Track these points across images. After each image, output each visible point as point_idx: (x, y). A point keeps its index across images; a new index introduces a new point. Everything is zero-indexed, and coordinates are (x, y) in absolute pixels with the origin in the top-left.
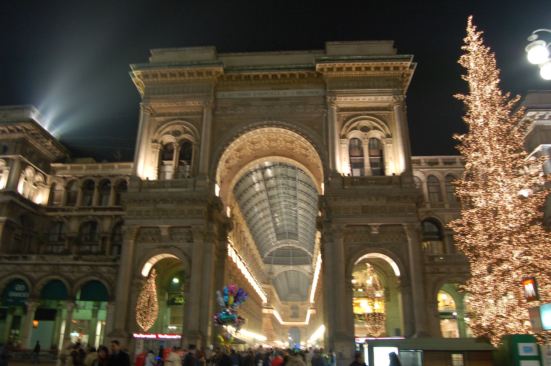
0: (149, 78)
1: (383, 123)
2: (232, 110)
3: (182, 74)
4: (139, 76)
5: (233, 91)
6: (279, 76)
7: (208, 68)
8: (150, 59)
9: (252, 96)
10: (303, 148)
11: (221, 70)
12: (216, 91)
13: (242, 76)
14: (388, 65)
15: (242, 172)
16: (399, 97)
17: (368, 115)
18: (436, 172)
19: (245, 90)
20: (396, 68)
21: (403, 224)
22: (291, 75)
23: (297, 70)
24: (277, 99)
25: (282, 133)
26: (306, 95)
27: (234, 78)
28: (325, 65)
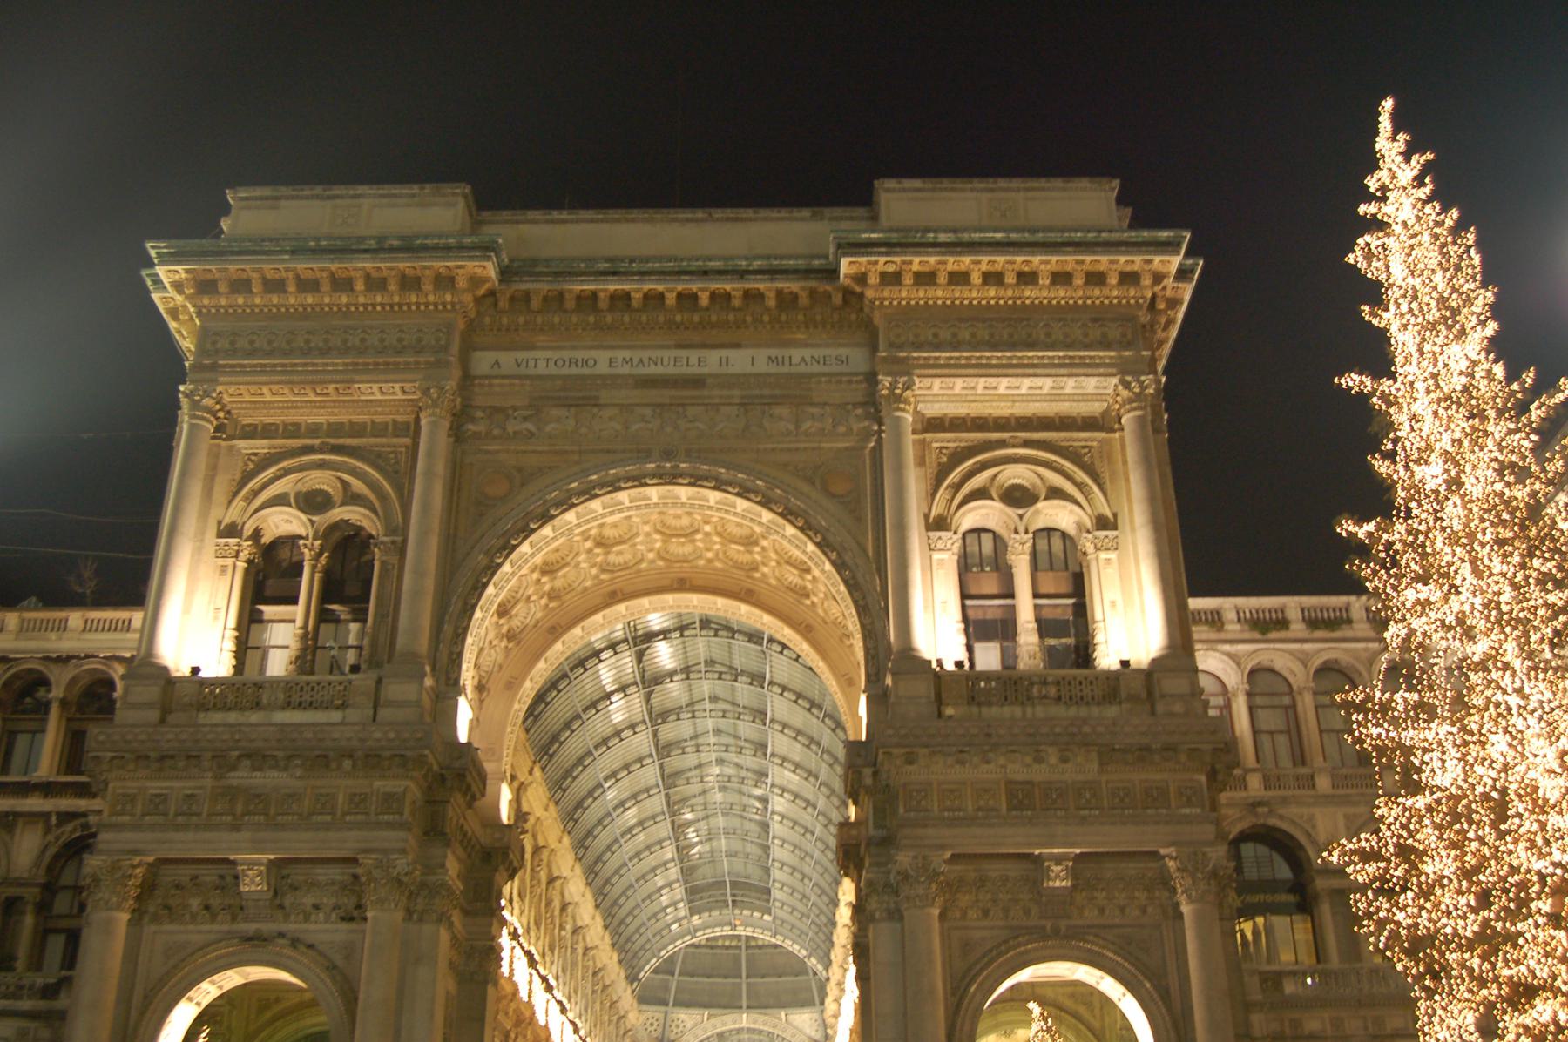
0: (218, 293)
1: (1081, 476)
2: (525, 419)
3: (342, 284)
4: (178, 286)
5: (533, 347)
6: (704, 300)
7: (439, 265)
8: (225, 224)
9: (603, 369)
10: (788, 563)
11: (490, 270)
12: (468, 348)
13: (567, 296)
14: (1102, 268)
15: (559, 652)
16: (1138, 381)
17: (1027, 444)
18: (1279, 655)
19: (574, 348)
20: (1129, 278)
21: (1163, 851)
22: (751, 296)
23: (772, 280)
24: (697, 382)
25: (710, 508)
26: (802, 369)
27: (535, 303)
28: (869, 263)
